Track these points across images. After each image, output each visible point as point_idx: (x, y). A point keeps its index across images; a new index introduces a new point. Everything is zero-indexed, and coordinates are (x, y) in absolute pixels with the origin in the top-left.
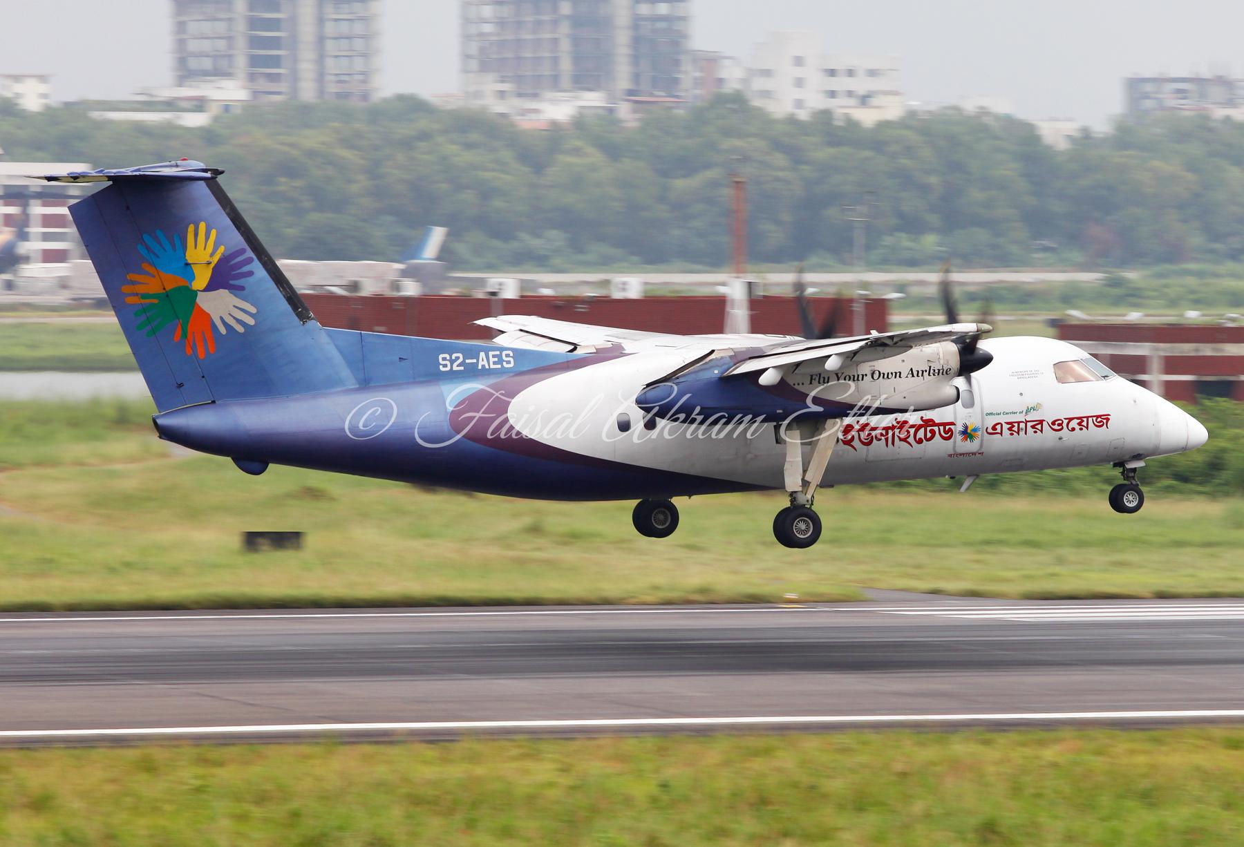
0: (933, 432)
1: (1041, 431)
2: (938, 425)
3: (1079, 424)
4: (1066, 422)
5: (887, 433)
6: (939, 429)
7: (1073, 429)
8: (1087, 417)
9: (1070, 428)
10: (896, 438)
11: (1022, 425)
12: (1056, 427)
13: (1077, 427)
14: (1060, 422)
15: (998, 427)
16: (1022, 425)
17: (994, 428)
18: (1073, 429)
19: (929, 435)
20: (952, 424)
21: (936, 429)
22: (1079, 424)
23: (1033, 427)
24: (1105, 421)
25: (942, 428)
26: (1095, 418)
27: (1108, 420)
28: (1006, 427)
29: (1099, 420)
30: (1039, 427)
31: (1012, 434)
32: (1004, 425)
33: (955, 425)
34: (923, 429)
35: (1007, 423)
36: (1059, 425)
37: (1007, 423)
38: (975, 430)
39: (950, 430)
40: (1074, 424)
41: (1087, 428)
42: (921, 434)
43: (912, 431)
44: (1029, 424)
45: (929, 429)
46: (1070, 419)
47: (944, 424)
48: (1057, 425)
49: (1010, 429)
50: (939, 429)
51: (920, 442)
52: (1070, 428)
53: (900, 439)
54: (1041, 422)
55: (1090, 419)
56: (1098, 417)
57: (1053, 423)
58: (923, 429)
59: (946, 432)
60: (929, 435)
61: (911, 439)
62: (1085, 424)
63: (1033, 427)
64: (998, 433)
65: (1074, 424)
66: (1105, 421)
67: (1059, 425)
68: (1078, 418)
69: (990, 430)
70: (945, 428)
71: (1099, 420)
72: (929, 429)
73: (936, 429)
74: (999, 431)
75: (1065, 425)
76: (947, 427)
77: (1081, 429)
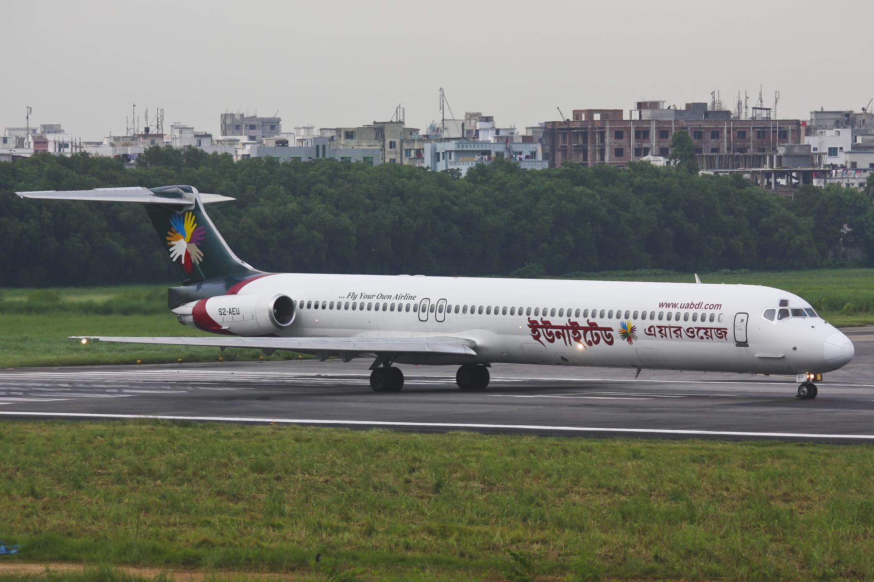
0: (597, 334)
2: (601, 329)
3: (706, 333)
4: (696, 330)
8: (711, 329)
11: (667, 329)
12: (690, 334)
13: (705, 337)
15: (652, 329)
16: (667, 329)
17: (650, 330)
20: (610, 329)
21: (599, 332)
23: (675, 332)
25: (603, 332)
27: (726, 333)
28: (657, 330)
29: (719, 332)
30: (678, 332)
33: (613, 331)
36: (692, 332)
38: (633, 329)
40: (702, 332)
43: (581, 332)
45: (594, 332)
46: (699, 329)
48: (692, 333)
54: (680, 328)
55: (713, 330)
56: (718, 329)
57: (688, 330)
60: (595, 339)
63: (675, 332)
65: (702, 332)
66: (723, 334)
67: (692, 332)
71: (719, 332)
73: (599, 332)
75: (695, 333)
76: (608, 332)
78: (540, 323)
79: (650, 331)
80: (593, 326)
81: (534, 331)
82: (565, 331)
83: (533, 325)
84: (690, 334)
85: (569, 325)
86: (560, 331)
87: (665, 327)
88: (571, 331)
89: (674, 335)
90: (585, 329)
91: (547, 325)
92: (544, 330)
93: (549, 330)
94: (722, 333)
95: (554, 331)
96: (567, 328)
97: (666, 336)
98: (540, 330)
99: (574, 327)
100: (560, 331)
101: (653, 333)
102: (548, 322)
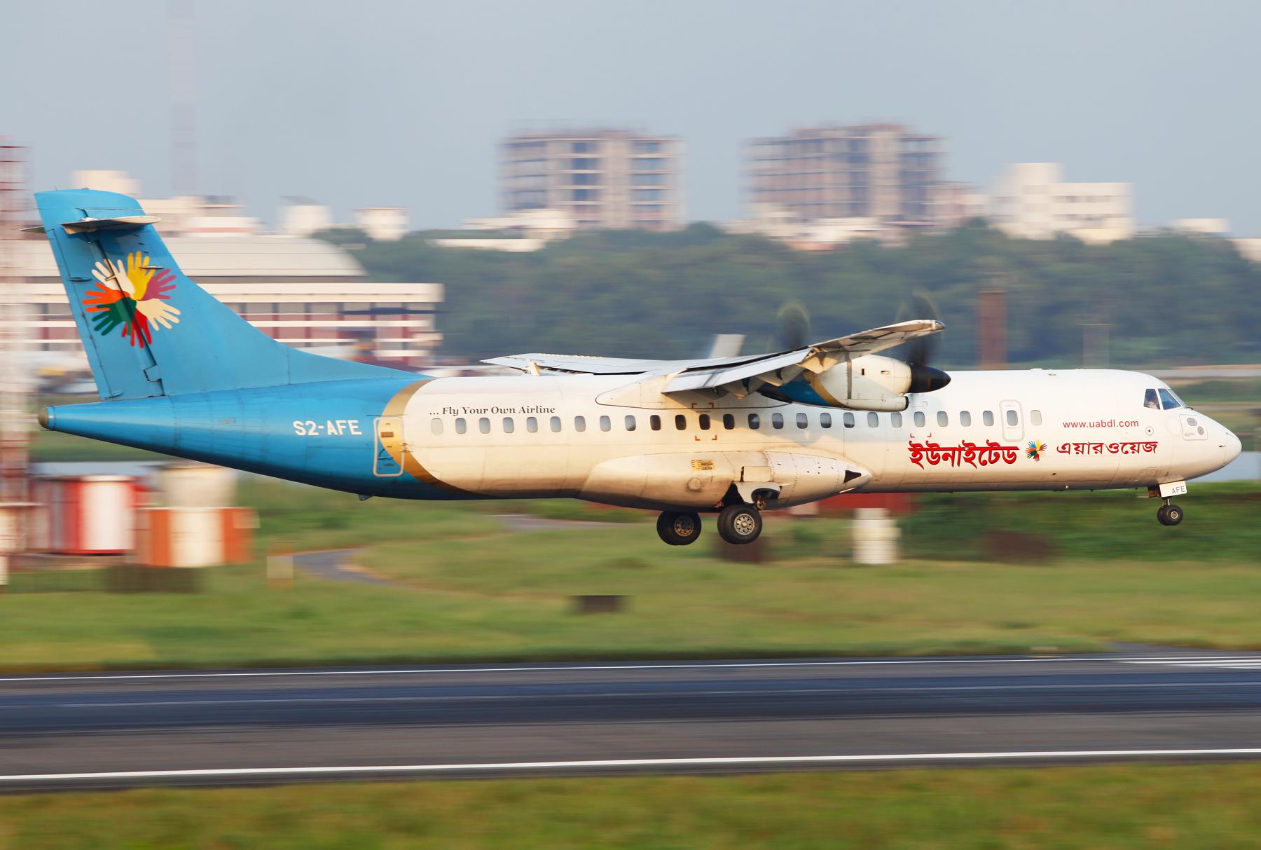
0: (997, 455)
1: (1101, 452)
3: (1132, 448)
4: (1121, 446)
5: (954, 454)
6: (1003, 453)
7: (1127, 452)
8: (1139, 443)
9: (1124, 451)
10: (962, 460)
11: (1086, 447)
12: (1113, 450)
13: (1130, 451)
14: (1116, 446)
15: (1067, 447)
16: (1086, 447)
17: (1063, 447)
18: (1127, 452)
19: (993, 458)
20: (1016, 448)
21: (1000, 452)
22: (1132, 448)
23: (1094, 448)
24: (1153, 447)
25: (1006, 452)
26: (1144, 445)
27: (1155, 446)
28: (1073, 447)
29: (1148, 446)
30: (1099, 448)
31: (1077, 453)
32: (1072, 445)
34: (988, 451)
35: (1074, 444)
36: (1115, 448)
37: (1074, 444)
38: (1042, 448)
39: (1014, 454)
40: (1127, 448)
41: (1138, 451)
42: (985, 456)
43: (977, 453)
44: (1092, 446)
45: (993, 452)
47: (1008, 449)
48: (1114, 448)
49: (1076, 449)
50: (1003, 453)
51: (984, 463)
52: (1124, 451)
53: (967, 460)
54: (1101, 445)
55: (1141, 445)
57: (1111, 446)
58: (988, 451)
59: (1009, 456)
61: (976, 461)
62: (1136, 448)
64: (1066, 452)
65: (1127, 448)
66: (1153, 447)
67: (1115, 448)
68: (1131, 444)
69: (1060, 449)
70: (1008, 452)
71: (1148, 446)
72: (993, 452)
74: (1067, 450)
75: (1120, 448)
76: (1011, 452)
77: (1133, 452)
78: (925, 446)
79: (1064, 449)
80: (993, 446)
81: (914, 455)
82: (957, 453)
83: (916, 449)
84: (1113, 450)
85: (962, 446)
86: (950, 452)
87: (1083, 444)
88: (963, 453)
89: (1092, 451)
90: (983, 450)
91: (933, 447)
92: (930, 453)
93: (935, 453)
94: (1151, 446)
95: (941, 453)
96: (960, 449)
97: (1082, 452)
98: (924, 453)
99: (971, 448)
100: (950, 452)
101: (1067, 450)
102: (936, 445)
